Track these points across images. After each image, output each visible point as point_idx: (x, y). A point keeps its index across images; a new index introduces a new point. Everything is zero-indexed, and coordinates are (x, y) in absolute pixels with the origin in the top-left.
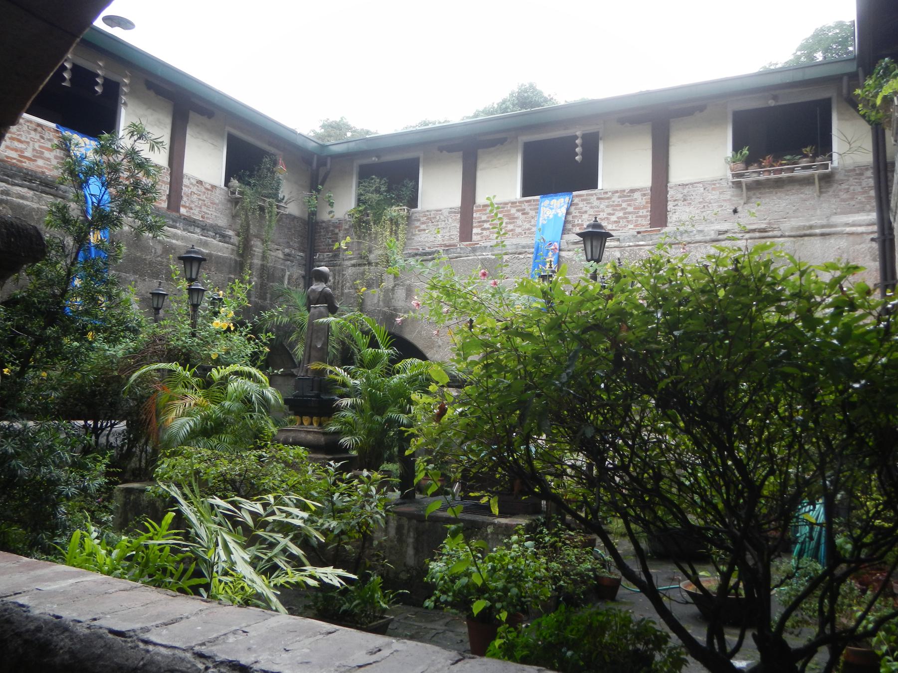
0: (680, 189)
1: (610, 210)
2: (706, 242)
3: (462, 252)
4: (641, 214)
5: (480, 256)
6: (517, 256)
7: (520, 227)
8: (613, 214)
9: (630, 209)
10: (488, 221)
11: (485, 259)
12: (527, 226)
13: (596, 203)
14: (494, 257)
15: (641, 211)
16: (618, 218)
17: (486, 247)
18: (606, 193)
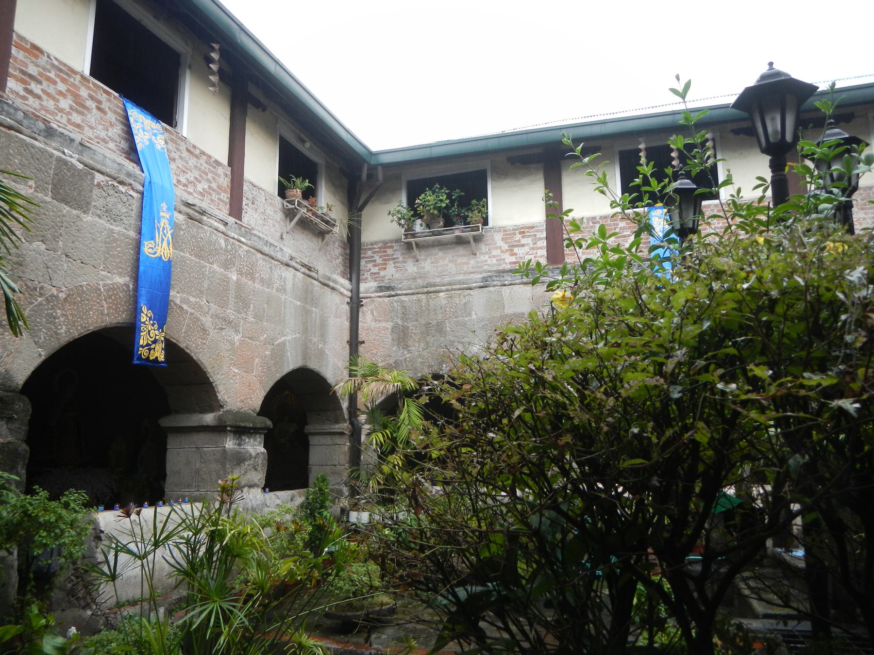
0: (251, 186)
1: (196, 174)
2: (282, 263)
3: (26, 122)
4: (222, 198)
5: (52, 148)
6: (116, 184)
7: (92, 128)
8: (200, 182)
9: (214, 185)
10: (40, 83)
11: (66, 163)
12: (103, 134)
13: (185, 154)
14: (81, 166)
15: (223, 194)
16: (204, 189)
17: (72, 140)
18: (194, 147)
